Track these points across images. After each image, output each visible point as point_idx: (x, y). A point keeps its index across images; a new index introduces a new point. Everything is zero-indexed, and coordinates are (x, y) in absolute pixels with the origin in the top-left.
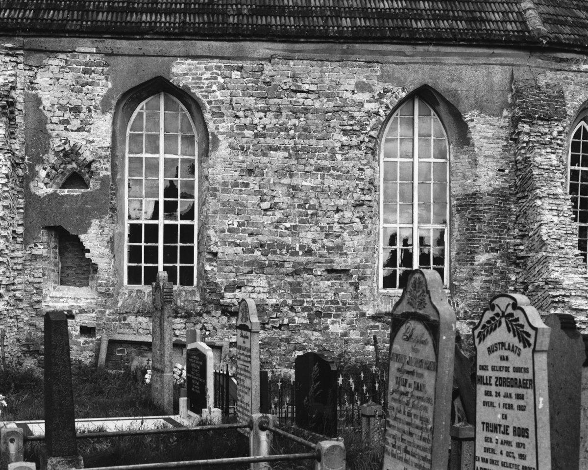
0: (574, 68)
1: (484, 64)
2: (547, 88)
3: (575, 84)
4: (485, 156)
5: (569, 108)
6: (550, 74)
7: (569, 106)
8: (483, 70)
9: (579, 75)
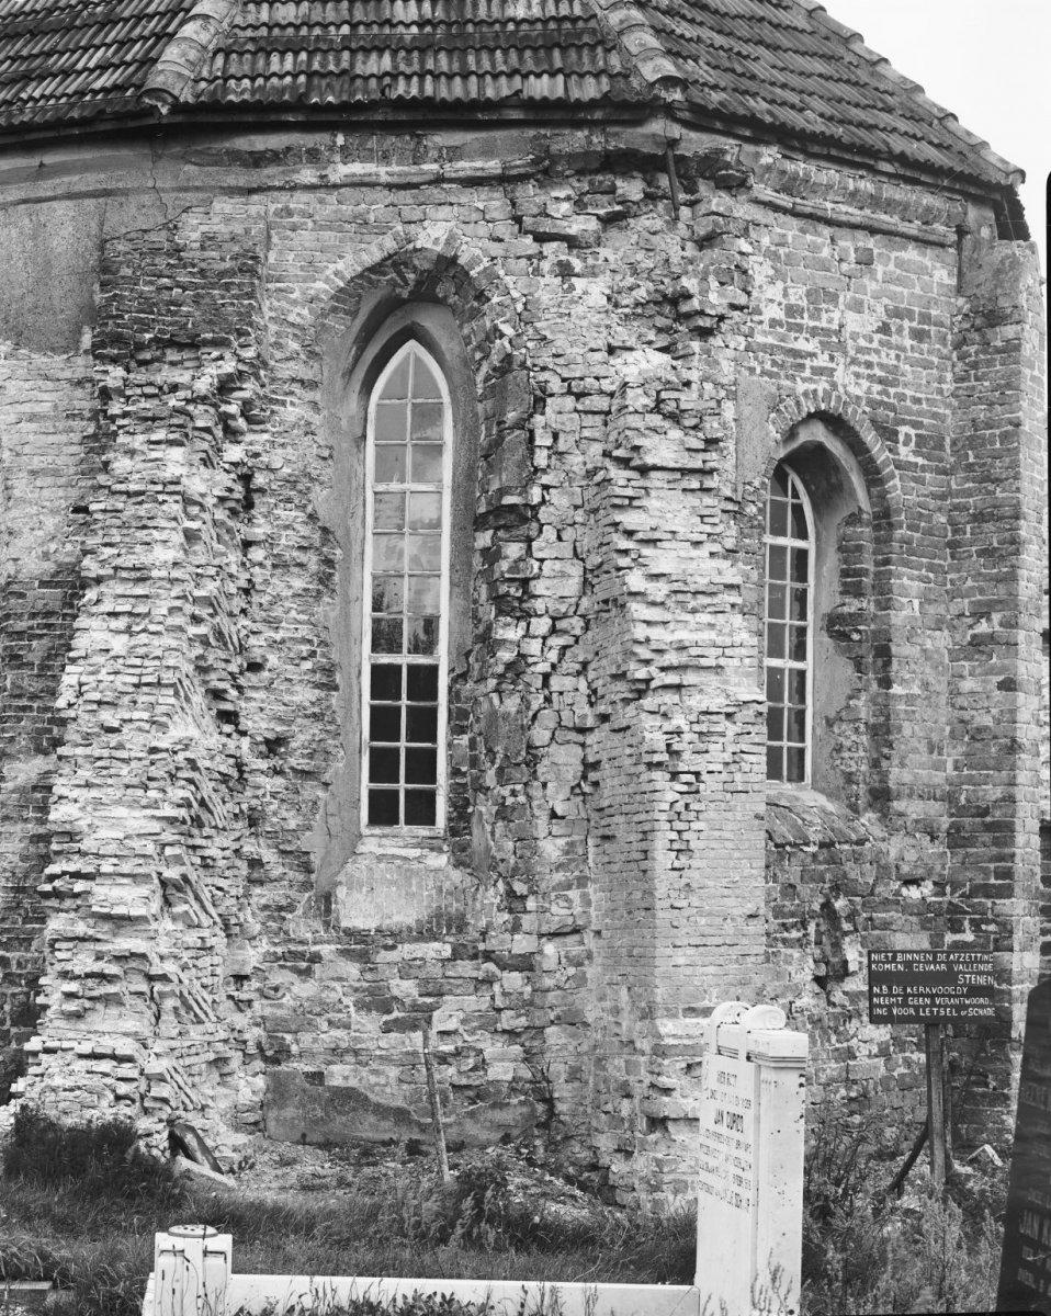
0: (307, 175)
1: (25, 201)
2: (203, 248)
3: (318, 227)
4: (33, 473)
5: (295, 302)
6: (223, 205)
8: (23, 218)
9: (332, 198)
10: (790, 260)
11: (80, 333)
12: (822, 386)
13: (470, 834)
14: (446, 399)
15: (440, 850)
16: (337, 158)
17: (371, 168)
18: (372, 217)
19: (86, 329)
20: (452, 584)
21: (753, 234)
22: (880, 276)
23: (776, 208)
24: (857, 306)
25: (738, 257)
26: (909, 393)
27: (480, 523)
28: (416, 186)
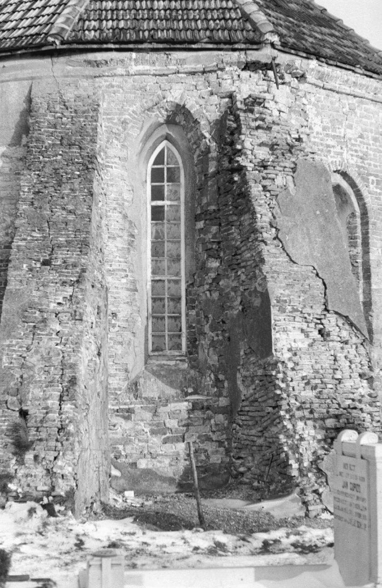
0: (120, 70)
5: (115, 124)
6: (85, 83)
7: (115, 121)
9: (130, 80)
10: (323, 108)
11: (21, 137)
12: (338, 159)
13: (198, 354)
14: (181, 165)
15: (184, 361)
16: (133, 63)
17: (147, 67)
18: (148, 88)
19: (24, 136)
20: (186, 245)
21: (308, 96)
22: (358, 115)
23: (317, 86)
24: (350, 127)
25: (303, 106)
26: (372, 163)
27: (197, 218)
28: (167, 75)
